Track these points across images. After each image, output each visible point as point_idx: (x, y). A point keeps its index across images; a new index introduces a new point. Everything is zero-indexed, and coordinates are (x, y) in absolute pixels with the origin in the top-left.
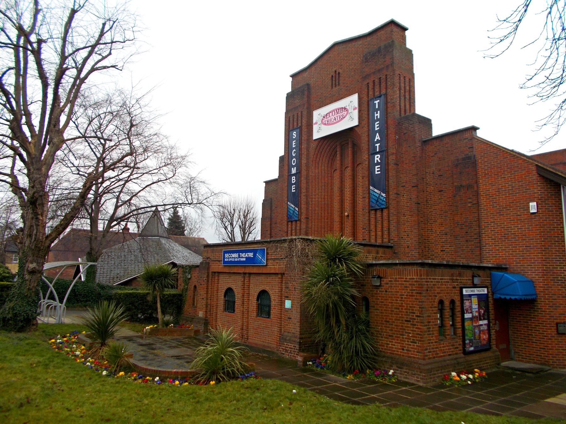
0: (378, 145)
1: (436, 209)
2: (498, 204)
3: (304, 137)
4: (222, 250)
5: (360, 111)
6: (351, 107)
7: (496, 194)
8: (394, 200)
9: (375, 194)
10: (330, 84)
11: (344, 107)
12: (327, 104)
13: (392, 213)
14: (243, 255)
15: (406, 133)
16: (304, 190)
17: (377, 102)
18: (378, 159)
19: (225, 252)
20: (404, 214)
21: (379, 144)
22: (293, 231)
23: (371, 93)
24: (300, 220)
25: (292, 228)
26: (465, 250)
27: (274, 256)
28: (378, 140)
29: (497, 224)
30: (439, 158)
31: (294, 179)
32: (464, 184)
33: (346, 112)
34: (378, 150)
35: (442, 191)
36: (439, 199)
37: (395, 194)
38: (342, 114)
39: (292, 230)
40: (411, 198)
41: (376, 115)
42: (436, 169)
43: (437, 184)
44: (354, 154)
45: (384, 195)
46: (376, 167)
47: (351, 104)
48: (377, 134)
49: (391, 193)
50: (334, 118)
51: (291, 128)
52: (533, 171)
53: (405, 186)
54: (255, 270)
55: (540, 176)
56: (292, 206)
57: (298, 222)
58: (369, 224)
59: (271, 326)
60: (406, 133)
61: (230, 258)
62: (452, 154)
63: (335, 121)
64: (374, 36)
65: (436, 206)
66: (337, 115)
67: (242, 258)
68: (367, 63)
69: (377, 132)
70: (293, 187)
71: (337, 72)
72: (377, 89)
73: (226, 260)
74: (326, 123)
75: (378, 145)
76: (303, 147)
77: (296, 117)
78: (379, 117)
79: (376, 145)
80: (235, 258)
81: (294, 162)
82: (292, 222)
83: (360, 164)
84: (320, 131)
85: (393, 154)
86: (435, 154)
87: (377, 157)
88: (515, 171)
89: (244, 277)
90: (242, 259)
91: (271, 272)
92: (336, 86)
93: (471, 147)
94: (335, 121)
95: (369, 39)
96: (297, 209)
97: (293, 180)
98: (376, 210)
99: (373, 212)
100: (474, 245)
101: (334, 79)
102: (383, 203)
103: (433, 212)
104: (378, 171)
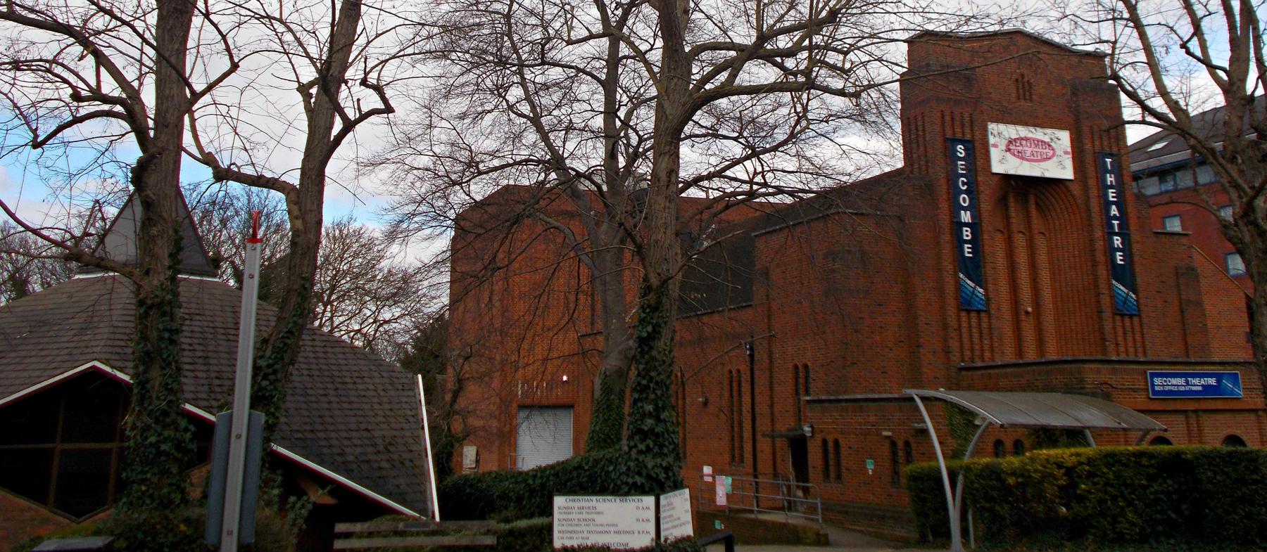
14: (1196, 381)
18: (1119, 242)
19: (1153, 375)
22: (974, 330)
24: (987, 312)
25: (969, 323)
39: (970, 327)
41: (1113, 179)
48: (1114, 207)
56: (969, 282)
57: (983, 315)
67: (1194, 385)
69: (1113, 203)
73: (1157, 388)
75: (1116, 222)
79: (1114, 222)
87: (1117, 240)
90: (1194, 388)
96: (981, 290)
97: (965, 233)
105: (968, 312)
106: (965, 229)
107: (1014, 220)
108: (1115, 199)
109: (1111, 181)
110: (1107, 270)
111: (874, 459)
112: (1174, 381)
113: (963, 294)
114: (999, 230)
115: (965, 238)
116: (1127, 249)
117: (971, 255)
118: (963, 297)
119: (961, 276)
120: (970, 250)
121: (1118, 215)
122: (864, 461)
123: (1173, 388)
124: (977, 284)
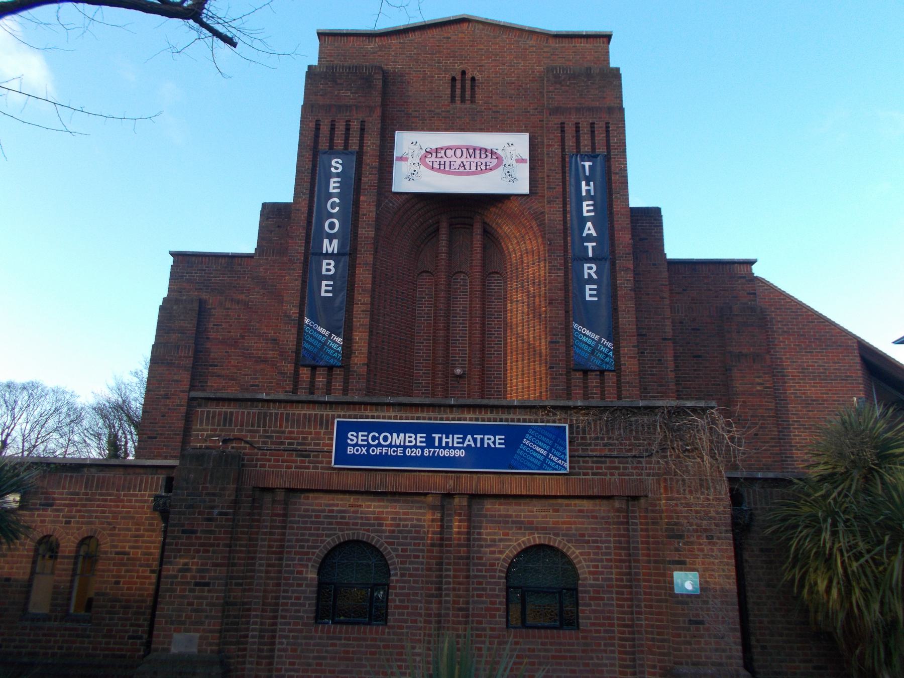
0: (590, 245)
1: (689, 388)
2: (804, 393)
3: (369, 178)
4: (333, 418)
5: (532, 169)
6: (509, 156)
7: (799, 376)
8: (631, 357)
9: (585, 339)
10: (449, 91)
11: (489, 148)
12: (438, 130)
13: (628, 383)
15: (647, 239)
16: (362, 299)
18: (592, 272)
20: (645, 389)
21: (594, 244)
23: (570, 142)
26: (752, 465)
27: (601, 450)
29: (805, 425)
30: (692, 300)
31: (328, 267)
32: (745, 351)
33: (495, 162)
34: (590, 255)
35: (699, 356)
36: (695, 370)
37: (633, 347)
38: (483, 161)
40: (660, 360)
42: (686, 316)
43: (689, 343)
44: (484, 248)
45: (609, 344)
46: (588, 287)
47: (507, 148)
48: (589, 224)
49: (623, 344)
50: (459, 162)
51: (323, 145)
52: (855, 349)
53: (644, 335)
54: (513, 486)
55: (863, 359)
57: (337, 371)
59: (584, 651)
60: (647, 239)
61: (379, 445)
62: (716, 297)
64: (566, 43)
65: (689, 381)
66: (470, 160)
68: (558, 86)
70: (325, 289)
71: (469, 76)
72: (585, 140)
73: (350, 450)
74: (436, 166)
75: (590, 245)
76: (362, 198)
77: (341, 128)
78: (592, 193)
79: (586, 244)
80: (405, 447)
82: (314, 368)
83: (497, 273)
85: (628, 269)
86: (684, 290)
88: (827, 346)
89: (442, 507)
90: (445, 453)
91: (590, 493)
92: (463, 100)
93: (752, 294)
94: (462, 169)
95: (553, 43)
96: (339, 340)
97: (324, 267)
98: (586, 372)
99: (579, 375)
100: (770, 457)
101: (458, 85)
102: (607, 359)
103: (682, 391)
105: (314, 368)
106: (325, 262)
108: (593, 214)
109: (588, 191)
112: (397, 439)
113: (306, 345)
114: (424, 272)
117: (330, 295)
118: (304, 348)
119: (307, 321)
121: (595, 234)
123: (390, 452)
124: (332, 332)
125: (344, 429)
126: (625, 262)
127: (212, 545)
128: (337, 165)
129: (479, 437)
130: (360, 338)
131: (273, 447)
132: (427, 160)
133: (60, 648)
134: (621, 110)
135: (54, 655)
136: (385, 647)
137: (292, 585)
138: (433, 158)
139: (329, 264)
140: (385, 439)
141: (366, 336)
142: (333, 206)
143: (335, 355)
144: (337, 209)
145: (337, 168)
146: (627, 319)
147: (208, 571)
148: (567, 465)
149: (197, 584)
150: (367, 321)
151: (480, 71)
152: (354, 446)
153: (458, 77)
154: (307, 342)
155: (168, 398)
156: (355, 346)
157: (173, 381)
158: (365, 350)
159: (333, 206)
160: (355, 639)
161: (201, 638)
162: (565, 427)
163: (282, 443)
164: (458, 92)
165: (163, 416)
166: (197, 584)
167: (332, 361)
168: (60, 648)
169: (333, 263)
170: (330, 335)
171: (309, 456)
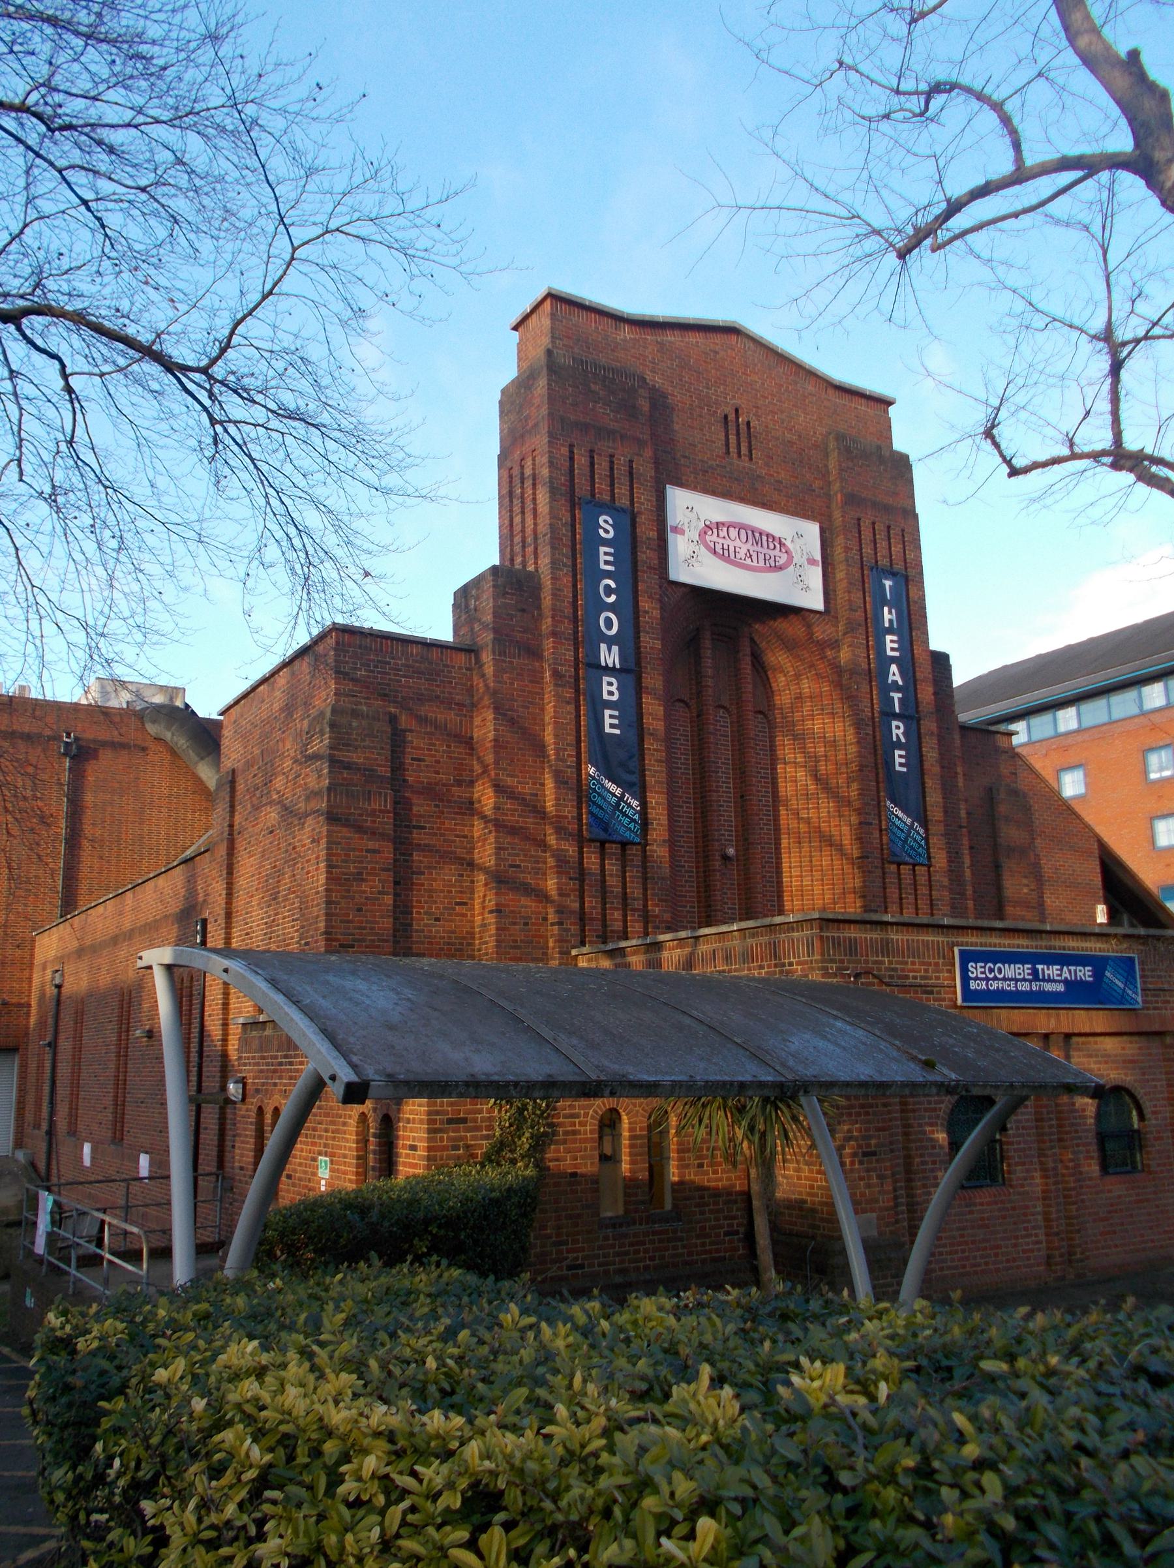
0: (897, 696)
4: (954, 944)
9: (898, 822)
10: (722, 436)
11: (777, 535)
14: (1053, 971)
17: (888, 583)
19: (966, 957)
24: (645, 845)
28: (896, 682)
31: (610, 689)
38: (772, 553)
48: (894, 668)
56: (609, 785)
57: (633, 851)
58: (885, 897)
61: (995, 978)
63: (748, 561)
64: (845, 400)
67: (1049, 980)
68: (850, 464)
69: (893, 660)
73: (973, 985)
75: (897, 696)
80: (1017, 980)
81: (611, 623)
82: (603, 843)
84: (693, 561)
87: (898, 727)
90: (1049, 987)
94: (748, 561)
96: (635, 803)
97: (605, 688)
104: (901, 765)
105: (603, 843)
106: (606, 679)
107: (710, 682)
109: (891, 621)
110: (878, 782)
111: (332, 1155)
112: (1010, 970)
113: (595, 810)
115: (606, 697)
116: (915, 746)
117: (617, 732)
120: (616, 722)
122: (315, 1160)
123: (1005, 986)
125: (966, 957)
126: (929, 725)
127: (871, 1106)
128: (606, 526)
129: (1072, 968)
130: (656, 800)
131: (900, 982)
132: (708, 538)
133: (652, 1259)
134: (916, 517)
135: (646, 1268)
136: (1014, 1209)
137: (926, 1148)
138: (714, 538)
139: (610, 684)
140: (1000, 971)
141: (663, 799)
142: (609, 591)
143: (632, 826)
144: (613, 598)
145: (607, 531)
146: (934, 798)
147: (870, 1137)
148: (1139, 999)
149: (865, 1154)
150: (663, 777)
151: (758, 416)
152: (976, 979)
153: (732, 417)
154: (594, 803)
155: (363, 880)
156: (652, 814)
157: (368, 851)
158: (664, 820)
159: (609, 591)
160: (988, 1204)
161: (878, 1218)
162: (1131, 960)
163: (907, 977)
164: (733, 438)
165: (360, 910)
166: (865, 1154)
167: (627, 834)
168: (652, 1259)
169: (613, 680)
170: (623, 795)
171: (932, 992)
